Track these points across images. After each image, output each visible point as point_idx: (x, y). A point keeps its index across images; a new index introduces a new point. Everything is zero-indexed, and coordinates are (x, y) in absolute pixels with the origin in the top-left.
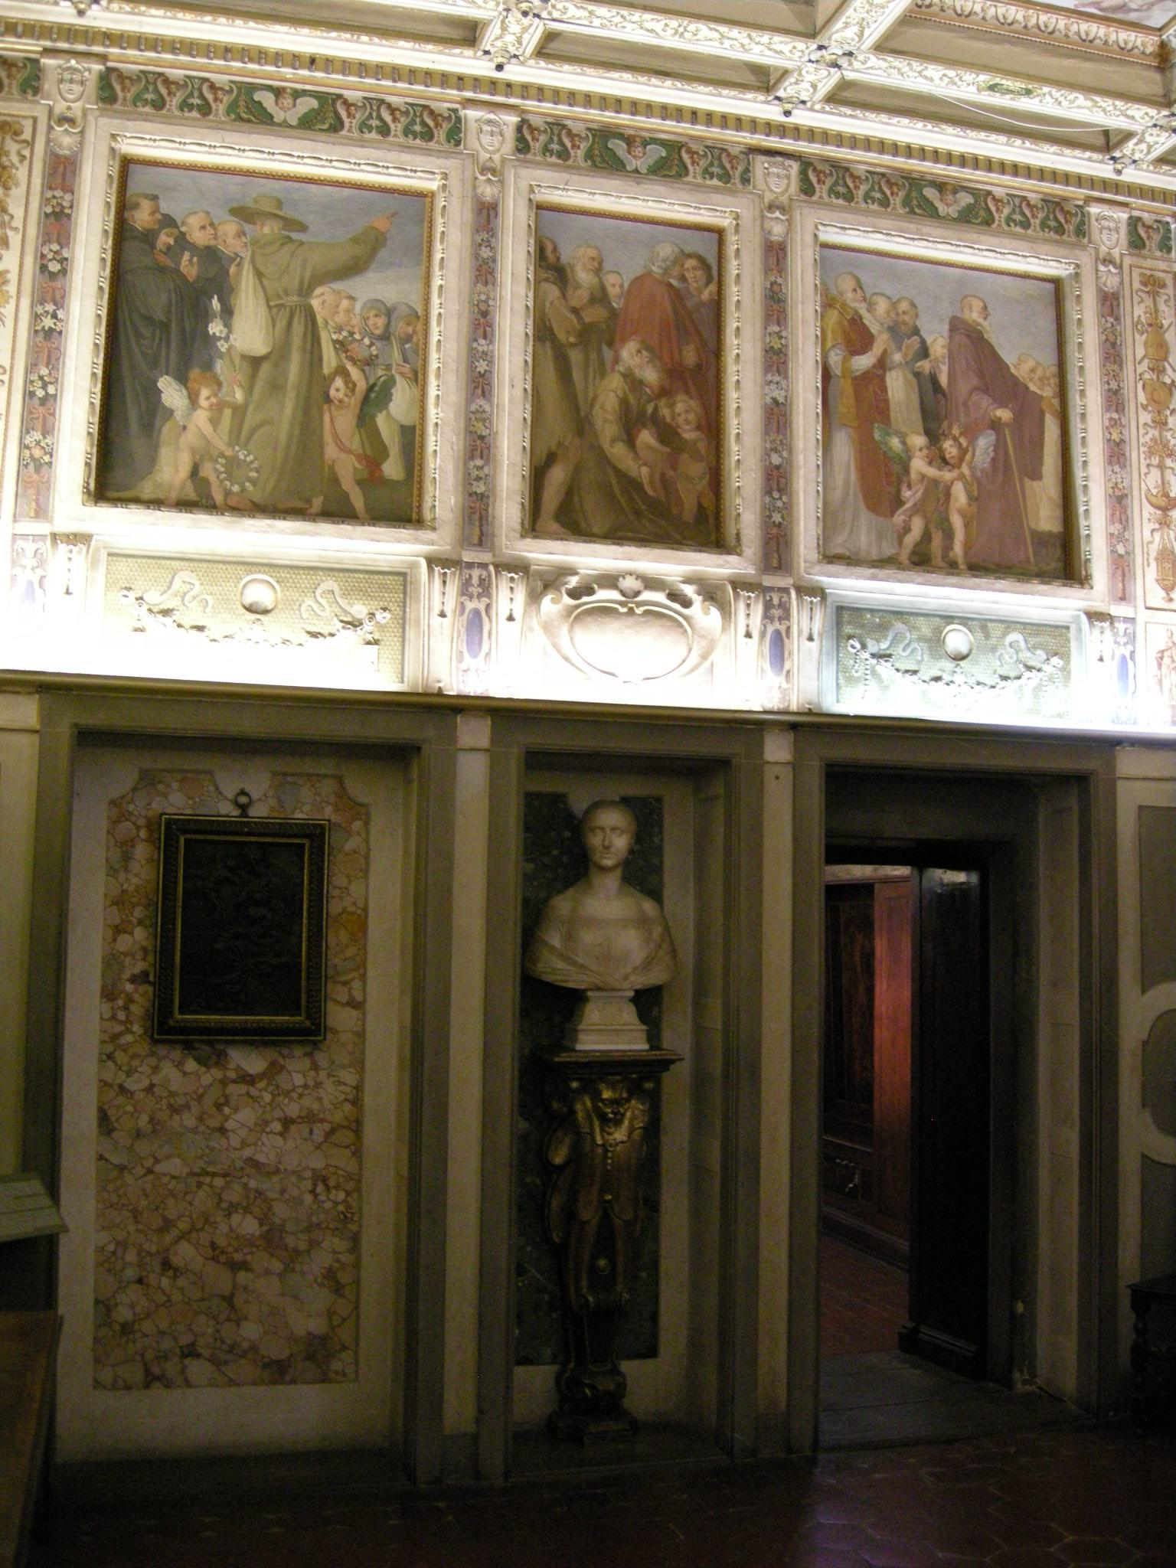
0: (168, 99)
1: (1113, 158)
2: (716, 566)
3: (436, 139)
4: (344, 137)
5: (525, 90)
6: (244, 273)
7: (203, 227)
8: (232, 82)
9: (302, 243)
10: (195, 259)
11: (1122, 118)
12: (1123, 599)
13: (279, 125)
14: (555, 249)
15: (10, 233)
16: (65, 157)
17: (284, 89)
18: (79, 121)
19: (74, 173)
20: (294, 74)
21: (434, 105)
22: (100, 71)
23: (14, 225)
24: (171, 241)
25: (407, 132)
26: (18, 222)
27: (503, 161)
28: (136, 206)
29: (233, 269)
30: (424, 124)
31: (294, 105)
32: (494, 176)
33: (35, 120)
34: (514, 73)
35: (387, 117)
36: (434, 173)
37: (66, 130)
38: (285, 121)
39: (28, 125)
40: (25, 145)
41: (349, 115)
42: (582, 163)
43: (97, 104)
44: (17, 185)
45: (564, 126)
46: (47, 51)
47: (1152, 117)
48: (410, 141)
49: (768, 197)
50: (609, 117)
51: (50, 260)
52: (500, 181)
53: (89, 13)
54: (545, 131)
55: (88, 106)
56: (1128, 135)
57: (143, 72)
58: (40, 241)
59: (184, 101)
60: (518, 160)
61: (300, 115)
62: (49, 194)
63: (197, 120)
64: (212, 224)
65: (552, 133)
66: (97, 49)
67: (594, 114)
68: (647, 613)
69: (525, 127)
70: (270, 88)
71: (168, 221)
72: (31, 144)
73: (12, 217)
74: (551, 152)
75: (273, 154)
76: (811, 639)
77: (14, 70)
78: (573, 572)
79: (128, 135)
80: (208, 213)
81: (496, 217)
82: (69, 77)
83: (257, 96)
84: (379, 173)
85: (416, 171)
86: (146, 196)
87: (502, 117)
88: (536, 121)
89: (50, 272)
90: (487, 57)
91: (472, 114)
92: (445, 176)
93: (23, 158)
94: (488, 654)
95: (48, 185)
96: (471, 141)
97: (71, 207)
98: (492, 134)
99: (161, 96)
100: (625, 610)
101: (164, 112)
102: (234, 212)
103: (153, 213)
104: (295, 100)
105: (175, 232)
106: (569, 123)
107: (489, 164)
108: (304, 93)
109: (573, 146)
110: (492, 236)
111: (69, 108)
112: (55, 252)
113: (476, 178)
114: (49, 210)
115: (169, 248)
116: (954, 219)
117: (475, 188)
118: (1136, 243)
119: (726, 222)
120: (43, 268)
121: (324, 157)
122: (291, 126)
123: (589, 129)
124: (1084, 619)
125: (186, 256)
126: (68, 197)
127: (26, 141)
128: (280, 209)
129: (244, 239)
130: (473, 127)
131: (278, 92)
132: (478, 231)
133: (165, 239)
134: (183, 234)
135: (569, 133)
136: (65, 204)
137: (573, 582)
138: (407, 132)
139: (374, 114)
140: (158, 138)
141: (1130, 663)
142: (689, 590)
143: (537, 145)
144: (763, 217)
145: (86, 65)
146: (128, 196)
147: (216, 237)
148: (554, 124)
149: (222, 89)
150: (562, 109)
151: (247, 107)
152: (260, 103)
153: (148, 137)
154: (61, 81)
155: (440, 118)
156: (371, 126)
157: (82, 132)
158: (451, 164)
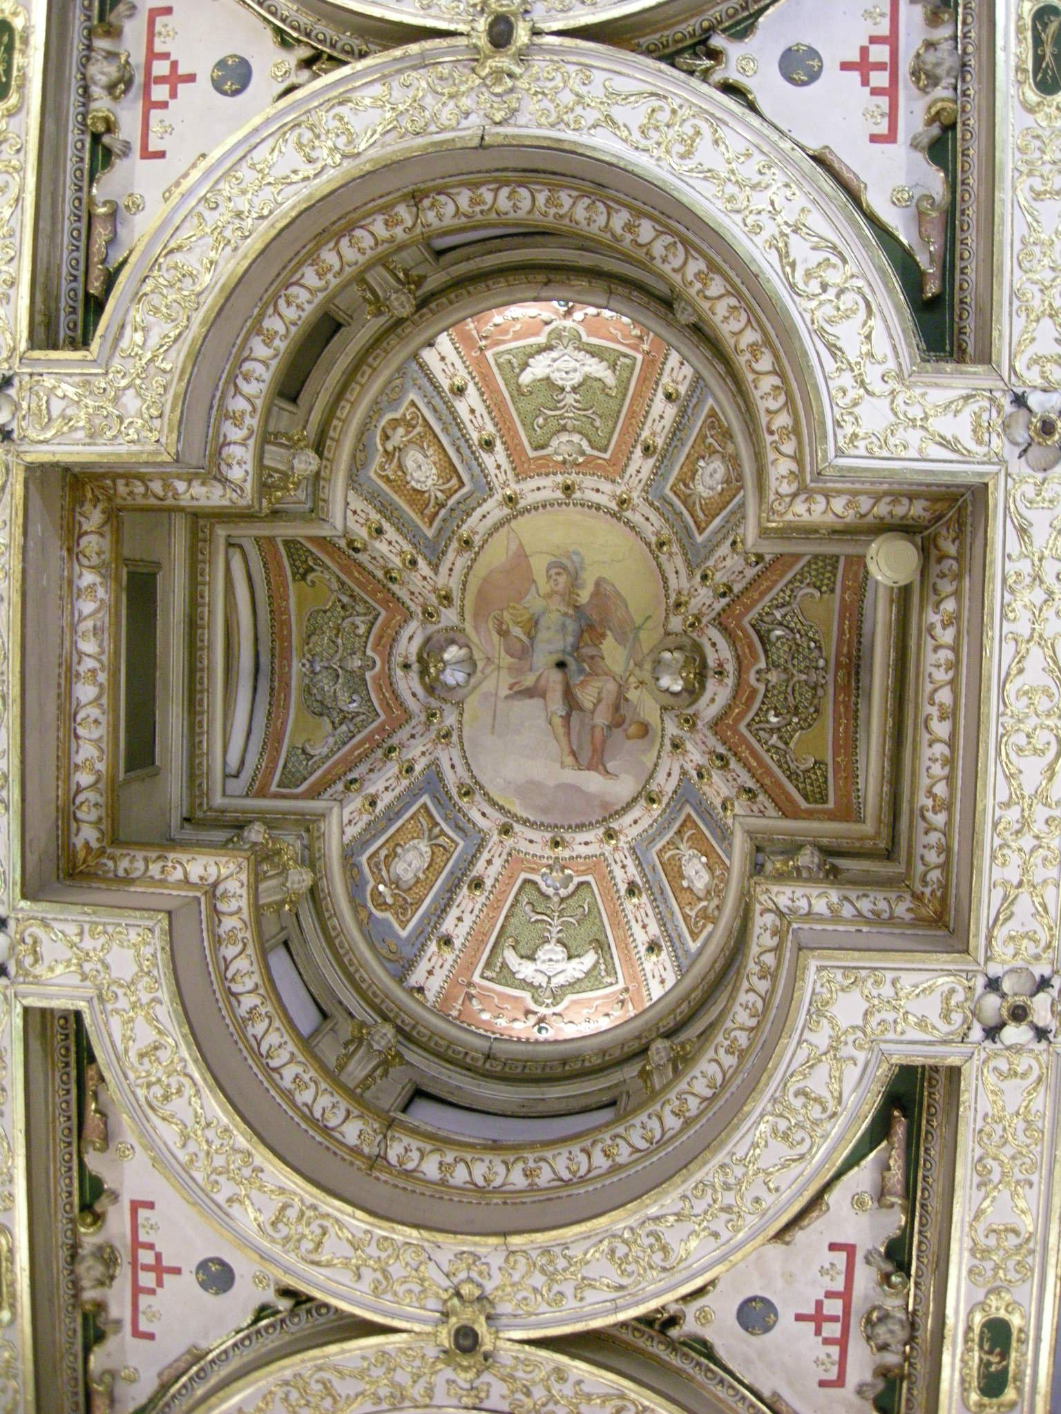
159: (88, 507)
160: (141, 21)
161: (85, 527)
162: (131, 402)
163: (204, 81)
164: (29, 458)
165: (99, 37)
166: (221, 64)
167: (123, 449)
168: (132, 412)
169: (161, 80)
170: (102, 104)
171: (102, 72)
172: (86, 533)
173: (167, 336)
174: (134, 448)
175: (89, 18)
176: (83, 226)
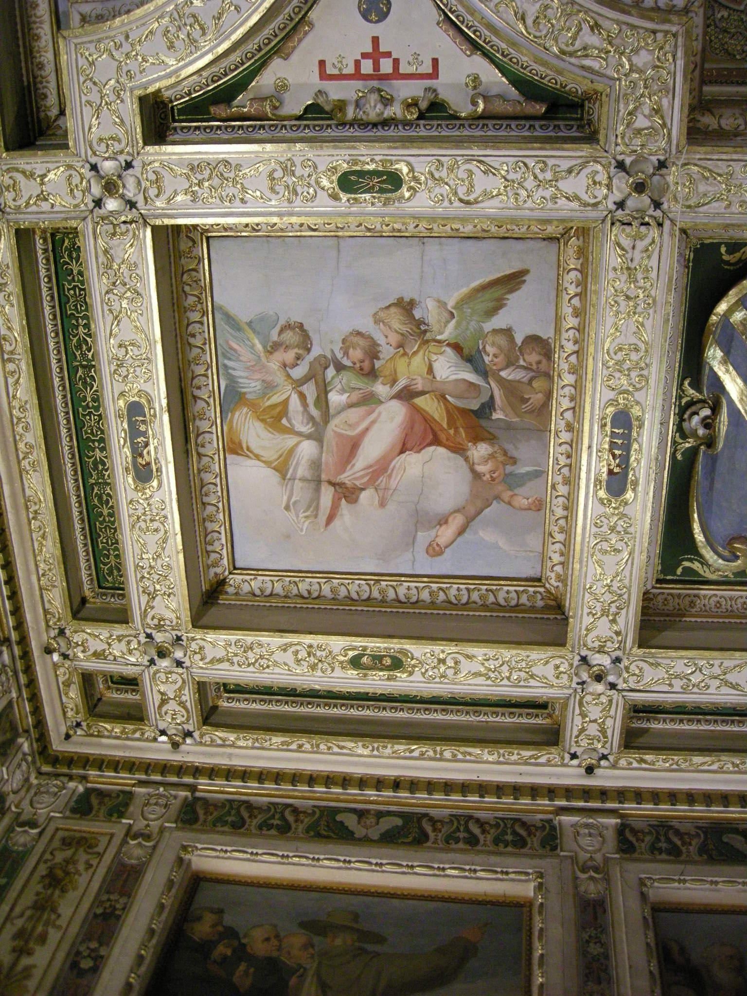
0: (248, 820)
3: (529, 845)
4: (429, 847)
5: (621, 794)
6: (307, 984)
7: (267, 939)
8: (314, 806)
9: (377, 954)
10: (252, 970)
13: (360, 840)
14: (682, 950)
15: (51, 931)
16: (132, 866)
17: (368, 811)
18: (155, 836)
19: (136, 880)
20: (378, 796)
21: (525, 818)
22: (186, 798)
23: (58, 923)
24: (229, 952)
25: (497, 841)
26: (62, 922)
27: (606, 860)
28: (199, 919)
29: (293, 981)
30: (515, 833)
31: (377, 824)
32: (598, 873)
33: (112, 835)
34: (605, 778)
35: (476, 831)
36: (527, 874)
37: (140, 844)
39: (104, 841)
40: (95, 856)
41: (434, 830)
42: (697, 858)
43: (176, 822)
44: (75, 889)
45: (671, 827)
46: (142, 783)
48: (501, 848)
50: (717, 812)
51: (85, 957)
52: (604, 879)
53: (183, 747)
54: (650, 833)
55: (167, 825)
57: (231, 801)
58: (80, 939)
59: (265, 821)
60: (621, 858)
61: (383, 831)
62: (105, 897)
63: (275, 836)
64: (277, 936)
65: (658, 833)
66: (188, 780)
67: (699, 810)
69: (627, 831)
70: (354, 811)
71: (231, 933)
72: (100, 855)
73: (59, 916)
74: (661, 851)
75: (350, 862)
77: (106, 800)
79: (200, 846)
80: (275, 926)
81: (605, 911)
82: (155, 801)
83: (339, 818)
84: (466, 877)
85: (507, 873)
86: (212, 911)
87: (599, 820)
88: (638, 825)
89: (80, 969)
90: (575, 762)
91: (567, 819)
92: (541, 875)
93: (89, 866)
95: (108, 886)
96: (568, 841)
97: (124, 909)
98: (590, 835)
99: (242, 818)
101: (242, 830)
102: (303, 925)
103: (214, 926)
105: (236, 943)
106: (675, 823)
107: (590, 863)
108: (389, 813)
109: (684, 844)
110: (602, 932)
111: (148, 825)
112: (92, 950)
113: (576, 878)
114: (99, 911)
115: (225, 958)
117: (576, 887)
120: (75, 965)
121: (405, 863)
123: (698, 827)
125: (243, 967)
126: (123, 900)
127: (99, 854)
128: (357, 922)
129: (311, 950)
130: (569, 832)
131: (361, 814)
132: (584, 928)
133: (222, 950)
134: (244, 945)
135: (677, 832)
136: (118, 906)
138: (497, 841)
139: (462, 828)
140: (229, 849)
143: (643, 845)
145: (173, 792)
146: (192, 909)
147: (279, 949)
148: (658, 826)
149: (305, 812)
150: (665, 809)
151: (328, 826)
152: (342, 823)
153: (219, 848)
154: (146, 805)
155: (532, 828)
156: (458, 837)
157: (154, 847)
158: (548, 864)
159: (699, 125)
160: (328, 85)
161: (716, 127)
162: (638, 60)
163: (377, 29)
164: (684, 141)
165: (345, 114)
166: (365, 16)
167: (680, 63)
168: (650, 58)
169: (376, 67)
170: (395, 110)
171: (374, 110)
172: (720, 126)
173: (592, 28)
174: (679, 54)
175: (329, 126)
176: (490, 123)
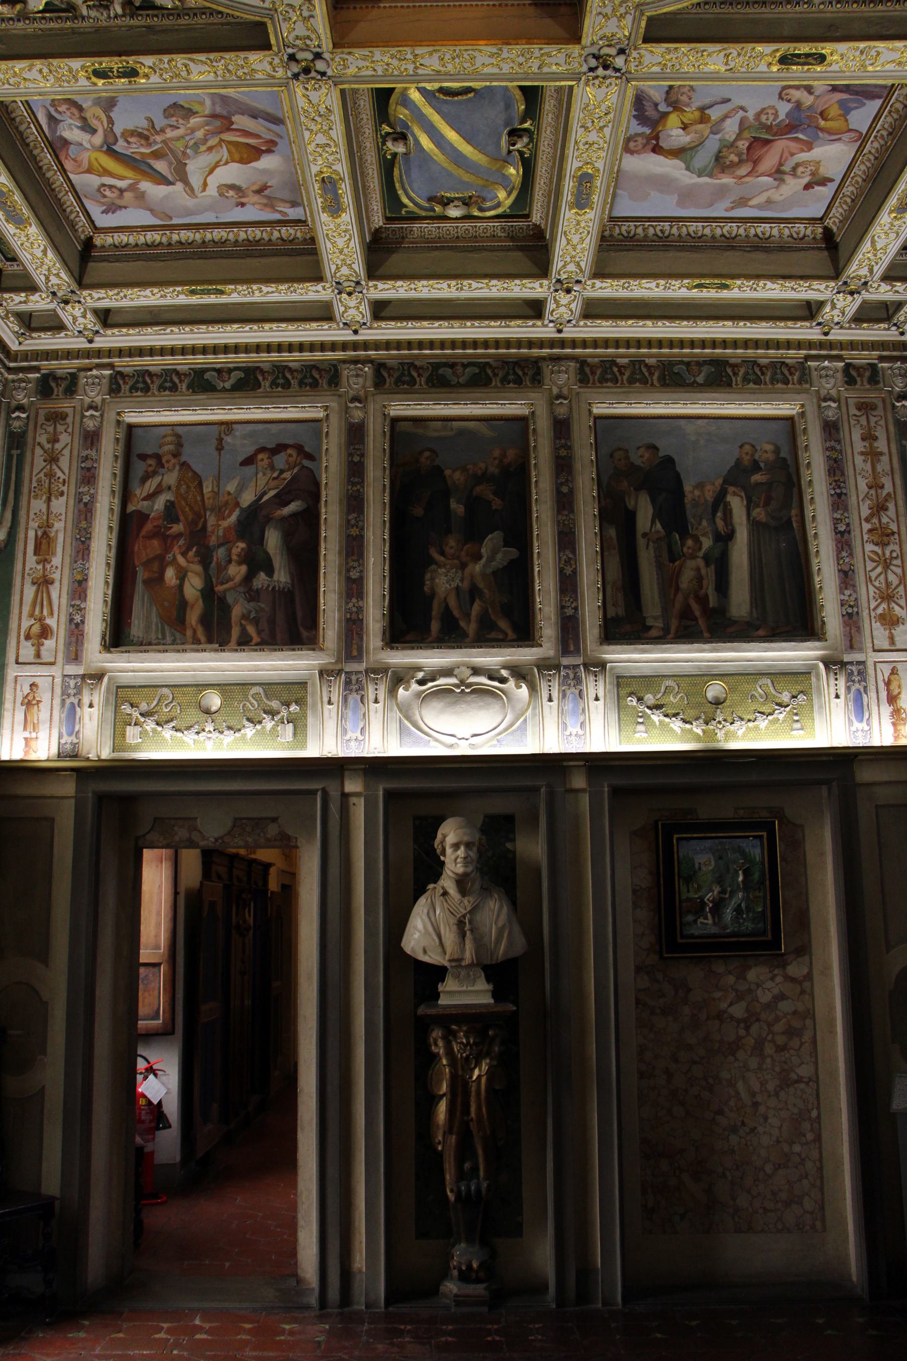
1: (819, 324)
2: (524, 655)
11: (810, 292)
12: (851, 647)
25: (301, 383)
38: (224, 387)
47: (833, 288)
49: (555, 391)
56: (821, 304)
68: (474, 692)
76: (597, 699)
78: (419, 669)
94: (362, 728)
100: (459, 691)
104: (230, 374)
108: (236, 369)
116: (701, 385)
118: (850, 381)
119: (526, 411)
122: (227, 390)
124: (821, 666)
131: (219, 371)
137: (420, 675)
138: (301, 383)
141: (865, 696)
142: (504, 673)
144: (552, 404)
